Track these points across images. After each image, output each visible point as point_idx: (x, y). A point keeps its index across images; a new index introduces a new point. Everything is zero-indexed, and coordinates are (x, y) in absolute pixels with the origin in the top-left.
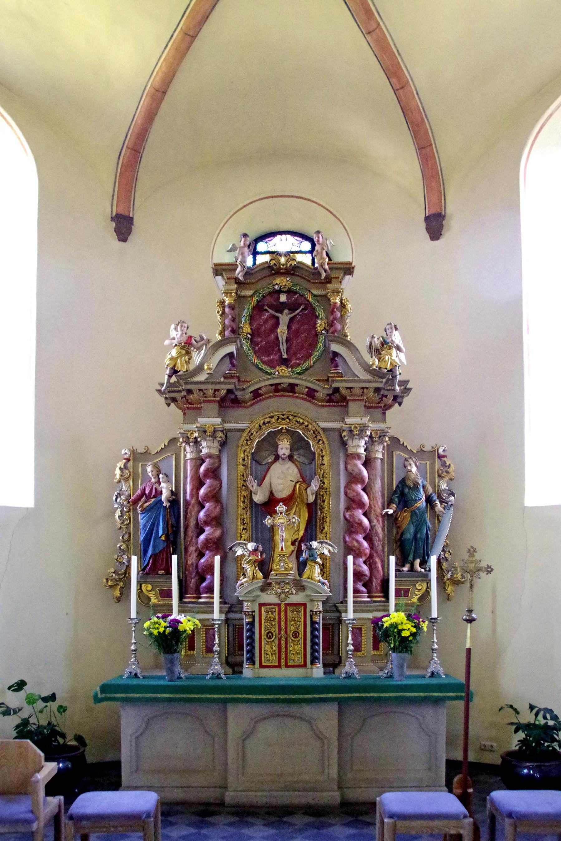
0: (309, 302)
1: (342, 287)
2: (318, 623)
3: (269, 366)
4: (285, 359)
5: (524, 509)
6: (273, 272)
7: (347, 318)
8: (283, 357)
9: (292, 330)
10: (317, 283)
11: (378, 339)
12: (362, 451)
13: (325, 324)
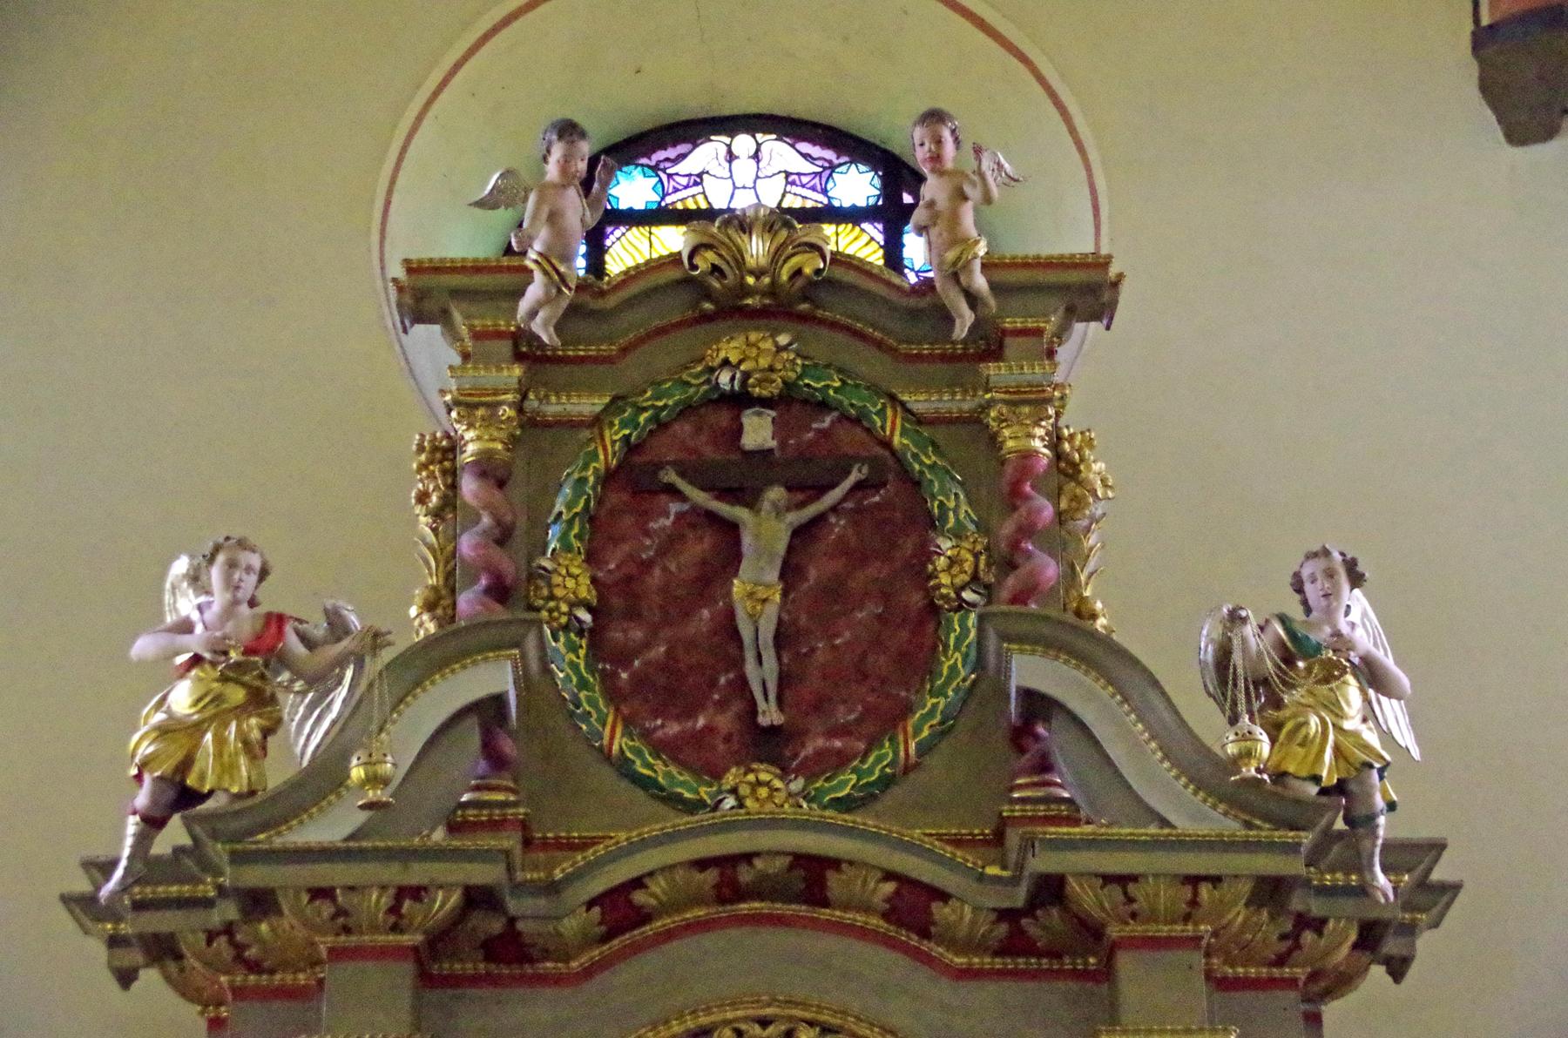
0: (893, 452)
1: (1058, 378)
3: (684, 765)
4: (773, 730)
6: (708, 306)
7: (1088, 530)
8: (763, 721)
9: (806, 585)
10: (931, 358)
11: (1262, 628)
13: (976, 556)
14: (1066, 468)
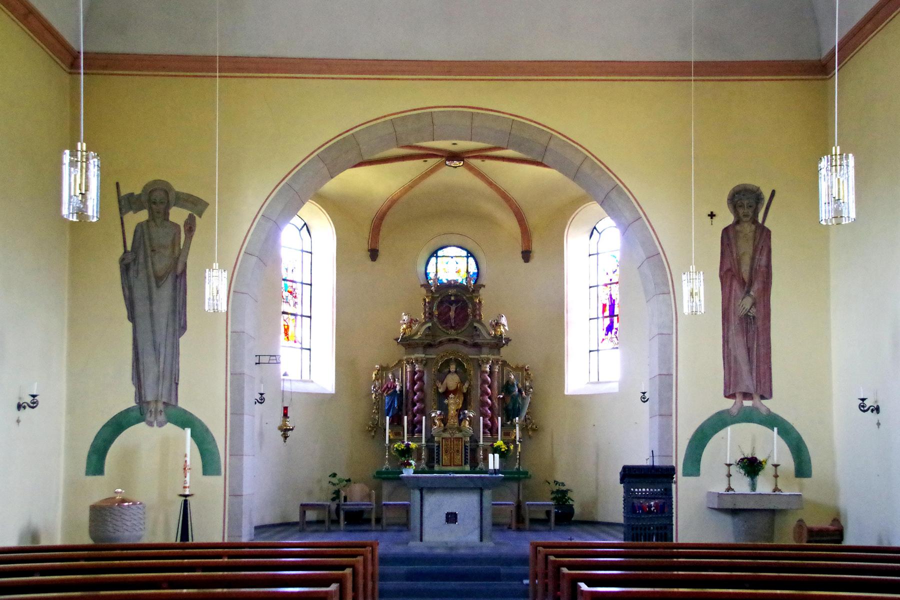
2: (468, 447)
5: (564, 395)
12: (488, 369)
14: (480, 302)
